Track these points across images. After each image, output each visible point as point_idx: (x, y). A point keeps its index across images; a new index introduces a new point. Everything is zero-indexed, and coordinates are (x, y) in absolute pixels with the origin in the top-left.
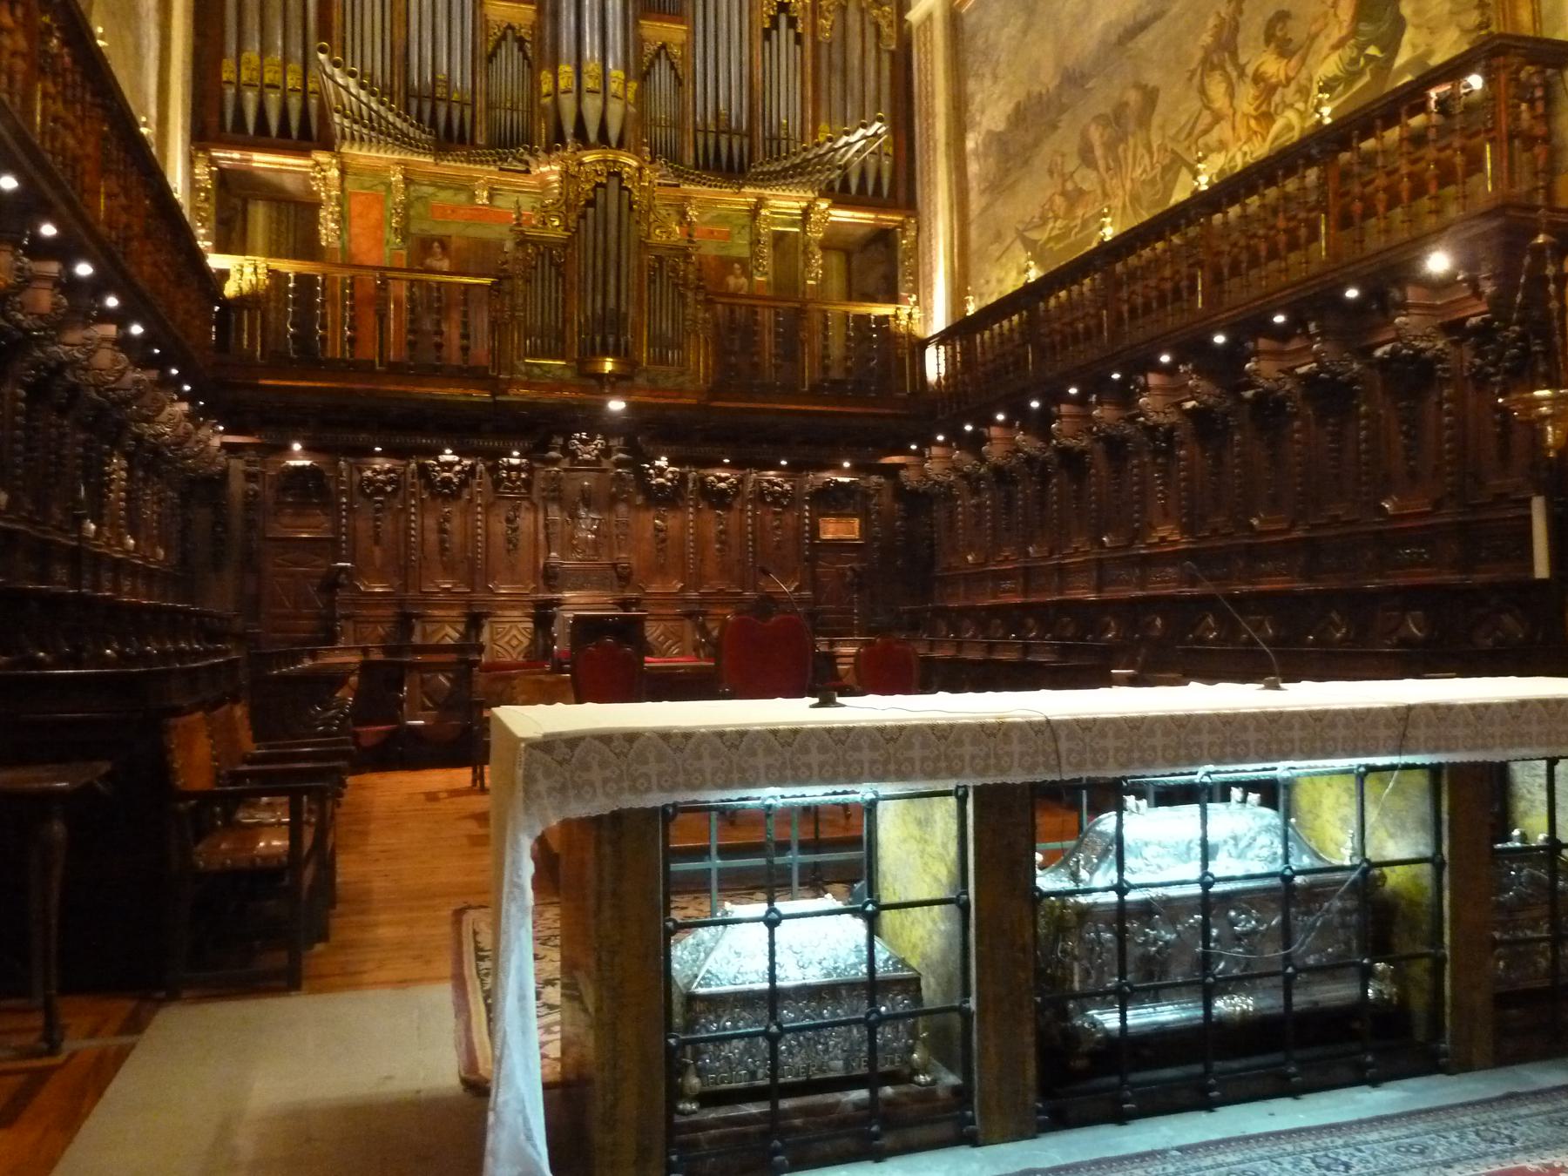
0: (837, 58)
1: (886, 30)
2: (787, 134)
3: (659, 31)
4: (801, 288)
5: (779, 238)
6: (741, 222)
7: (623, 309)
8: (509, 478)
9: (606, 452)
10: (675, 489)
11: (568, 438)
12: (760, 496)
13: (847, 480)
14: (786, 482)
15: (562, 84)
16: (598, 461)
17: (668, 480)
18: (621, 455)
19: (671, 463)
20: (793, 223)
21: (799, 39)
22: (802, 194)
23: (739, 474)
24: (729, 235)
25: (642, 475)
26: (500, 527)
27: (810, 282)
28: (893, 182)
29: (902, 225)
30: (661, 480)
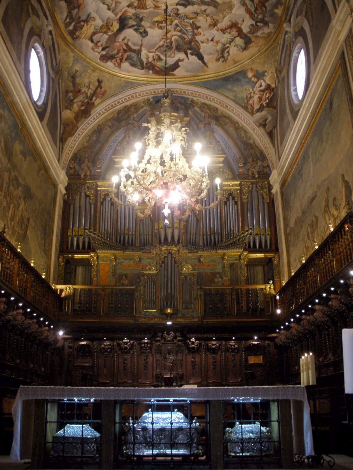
0: (249, 207)
1: (265, 197)
2: (233, 232)
4: (240, 280)
5: (232, 265)
6: (219, 261)
8: (144, 346)
9: (175, 337)
10: (198, 348)
11: (163, 333)
12: (227, 350)
13: (256, 343)
14: (236, 344)
16: (173, 340)
17: (195, 345)
18: (180, 338)
19: (196, 339)
20: (236, 260)
21: (236, 203)
22: (238, 250)
23: (219, 342)
24: (215, 265)
25: (187, 344)
26: (142, 362)
27: (242, 278)
28: (271, 244)
29: (274, 257)
30: (193, 346)
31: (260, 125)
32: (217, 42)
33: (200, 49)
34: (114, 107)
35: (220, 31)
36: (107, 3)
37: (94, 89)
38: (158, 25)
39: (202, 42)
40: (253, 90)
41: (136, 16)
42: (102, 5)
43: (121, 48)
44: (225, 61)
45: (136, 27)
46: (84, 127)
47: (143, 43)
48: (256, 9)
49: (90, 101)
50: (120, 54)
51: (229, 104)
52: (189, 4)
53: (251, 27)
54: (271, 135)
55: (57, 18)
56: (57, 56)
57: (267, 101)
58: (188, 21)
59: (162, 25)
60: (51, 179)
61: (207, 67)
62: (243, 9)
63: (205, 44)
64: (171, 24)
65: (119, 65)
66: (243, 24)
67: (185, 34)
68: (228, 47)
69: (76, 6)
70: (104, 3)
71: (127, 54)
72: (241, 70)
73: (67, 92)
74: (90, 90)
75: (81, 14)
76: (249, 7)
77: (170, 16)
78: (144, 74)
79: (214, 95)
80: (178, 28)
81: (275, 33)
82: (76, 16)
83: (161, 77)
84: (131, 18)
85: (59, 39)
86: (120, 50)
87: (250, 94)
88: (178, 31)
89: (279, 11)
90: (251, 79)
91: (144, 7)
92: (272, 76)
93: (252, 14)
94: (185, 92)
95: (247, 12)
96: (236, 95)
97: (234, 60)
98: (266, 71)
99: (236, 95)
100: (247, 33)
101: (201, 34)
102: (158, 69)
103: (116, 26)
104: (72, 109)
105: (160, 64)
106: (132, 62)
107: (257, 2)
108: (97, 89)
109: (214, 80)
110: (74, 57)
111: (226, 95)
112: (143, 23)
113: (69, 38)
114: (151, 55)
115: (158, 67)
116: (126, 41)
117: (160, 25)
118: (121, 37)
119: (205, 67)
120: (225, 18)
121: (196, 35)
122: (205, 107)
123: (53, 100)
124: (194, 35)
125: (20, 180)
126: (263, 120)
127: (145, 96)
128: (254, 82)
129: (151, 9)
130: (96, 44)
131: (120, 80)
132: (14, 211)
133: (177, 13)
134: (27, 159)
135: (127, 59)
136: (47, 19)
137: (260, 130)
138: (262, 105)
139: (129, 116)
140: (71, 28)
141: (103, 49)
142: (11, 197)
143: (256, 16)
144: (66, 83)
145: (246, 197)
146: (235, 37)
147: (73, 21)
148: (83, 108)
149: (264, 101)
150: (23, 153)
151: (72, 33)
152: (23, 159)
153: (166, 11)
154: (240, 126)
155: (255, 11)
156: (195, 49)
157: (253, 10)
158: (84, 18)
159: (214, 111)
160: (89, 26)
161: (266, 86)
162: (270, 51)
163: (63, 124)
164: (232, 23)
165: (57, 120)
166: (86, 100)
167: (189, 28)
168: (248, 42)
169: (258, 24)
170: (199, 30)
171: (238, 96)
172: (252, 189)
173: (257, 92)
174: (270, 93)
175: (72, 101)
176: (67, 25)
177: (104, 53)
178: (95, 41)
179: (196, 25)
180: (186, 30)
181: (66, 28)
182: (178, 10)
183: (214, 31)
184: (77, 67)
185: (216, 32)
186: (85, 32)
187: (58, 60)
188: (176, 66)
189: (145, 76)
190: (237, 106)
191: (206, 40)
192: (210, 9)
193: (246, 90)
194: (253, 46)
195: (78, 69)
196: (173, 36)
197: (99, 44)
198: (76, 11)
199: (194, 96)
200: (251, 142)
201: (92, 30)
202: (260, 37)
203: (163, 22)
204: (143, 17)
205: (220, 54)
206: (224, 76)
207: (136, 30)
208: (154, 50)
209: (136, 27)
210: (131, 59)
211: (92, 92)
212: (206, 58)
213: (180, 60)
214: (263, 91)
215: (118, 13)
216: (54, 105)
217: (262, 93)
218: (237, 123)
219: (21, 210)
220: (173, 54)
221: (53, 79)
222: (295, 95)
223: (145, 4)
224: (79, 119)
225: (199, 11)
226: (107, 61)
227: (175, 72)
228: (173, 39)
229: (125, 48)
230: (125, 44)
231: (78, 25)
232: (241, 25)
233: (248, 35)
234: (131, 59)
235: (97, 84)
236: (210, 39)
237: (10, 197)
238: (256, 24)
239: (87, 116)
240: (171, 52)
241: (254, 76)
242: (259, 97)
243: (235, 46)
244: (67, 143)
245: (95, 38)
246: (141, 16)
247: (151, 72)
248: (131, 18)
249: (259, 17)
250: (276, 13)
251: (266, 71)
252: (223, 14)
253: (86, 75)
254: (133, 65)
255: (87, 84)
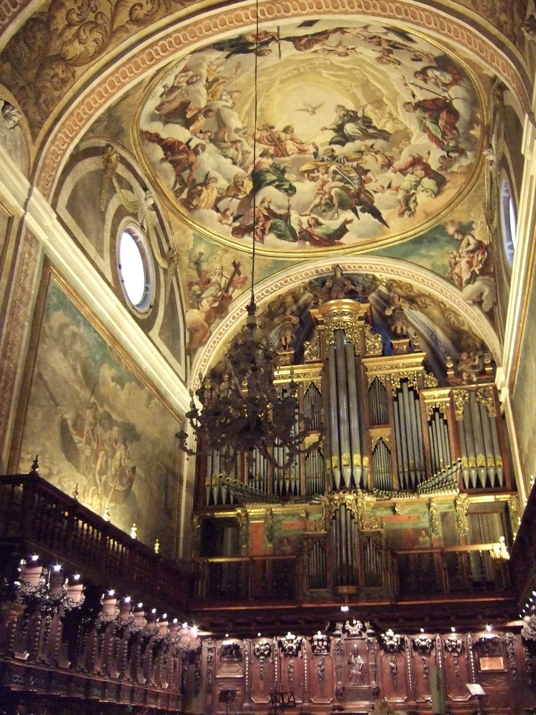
3: (377, 433)
7: (350, 563)
15: (334, 465)
31: (474, 303)
32: (397, 189)
33: (373, 202)
34: (262, 298)
35: (398, 173)
36: (231, 156)
37: (229, 277)
38: (308, 175)
39: (375, 192)
40: (458, 252)
41: (276, 168)
42: (223, 159)
43: (261, 215)
44: (412, 214)
45: (277, 183)
46: (221, 330)
47: (290, 203)
48: (444, 134)
49: (225, 295)
50: (261, 224)
51: (426, 276)
52: (348, 141)
53: (442, 161)
54: (491, 316)
55: (161, 185)
56: (170, 237)
57: (481, 266)
58: (350, 164)
59: (314, 175)
60: (171, 408)
61: (387, 226)
62: (426, 136)
63: (379, 195)
64: (327, 172)
65: (260, 238)
66: (429, 157)
67: (348, 183)
68: (414, 194)
69: (186, 165)
70: (226, 156)
71: (271, 221)
72: (437, 225)
73: (191, 284)
74: (224, 279)
75: (195, 175)
76: (433, 132)
77: (323, 160)
78: (298, 248)
79: (401, 266)
80: (338, 177)
81: (477, 164)
82: (188, 180)
83: (323, 249)
84: (268, 171)
85: (170, 214)
86: (260, 217)
87: (455, 258)
88: (338, 181)
89: (476, 132)
90: (453, 236)
91: (285, 153)
92: (482, 228)
93: (440, 141)
94: (360, 267)
95: (432, 141)
96: (434, 263)
97: (425, 212)
98: (473, 222)
99: (434, 263)
100: (438, 169)
101: (371, 180)
102: (318, 239)
103: (249, 185)
104: (200, 307)
105: (318, 231)
106: (279, 233)
107: (444, 124)
108: (233, 276)
109: (400, 244)
110: (194, 235)
111: (420, 264)
112: (286, 176)
113: (183, 210)
114: (304, 219)
115: (317, 236)
116: (266, 205)
117: (311, 175)
118: (259, 198)
119: (385, 227)
120: (403, 153)
121: (365, 182)
122: (394, 285)
123: (167, 299)
124: (362, 182)
125: (114, 417)
126: (477, 295)
127: (304, 278)
128: (457, 240)
129: (295, 155)
130: (224, 214)
131: (265, 260)
132: (106, 461)
133: (333, 155)
134: (126, 387)
135: (271, 229)
136: (145, 189)
137: (474, 310)
138: (473, 272)
139: (285, 310)
140: (184, 196)
141: (235, 220)
142: (100, 442)
143: (445, 143)
144: (187, 272)
145: (460, 412)
146: (421, 179)
147: (186, 186)
148: (216, 305)
149: (476, 267)
150: (119, 381)
151: (187, 203)
152: (118, 387)
153: (316, 155)
154: (448, 306)
155: (443, 137)
156: (366, 203)
157: (440, 136)
158: (200, 179)
159: (406, 289)
160: (209, 190)
161: (476, 244)
162: (475, 191)
163: (190, 330)
164: (414, 159)
165: (178, 324)
166: (220, 294)
167: (354, 174)
168: (441, 182)
169: (451, 154)
170: (369, 175)
171: (436, 264)
172: (469, 399)
173: (464, 254)
174: (483, 254)
175: (199, 296)
176: (178, 193)
177: (237, 224)
178: (222, 210)
179: (363, 169)
180: (350, 178)
181: (178, 197)
182: (333, 151)
183: (390, 174)
184: (201, 248)
185: (393, 174)
186: (206, 199)
187: (171, 242)
188: (342, 231)
189: (300, 251)
190: (438, 278)
191: (381, 188)
192: (379, 143)
193: (448, 253)
194: (449, 188)
195: (202, 251)
196: (332, 188)
197: (228, 213)
198: (187, 172)
199: (375, 271)
200: (466, 328)
201: (215, 195)
202: (457, 173)
203: (316, 171)
204: (285, 167)
205: (403, 206)
206: (413, 237)
207: (277, 187)
208: (308, 212)
209: (277, 183)
210: (277, 229)
211: (227, 281)
212: (384, 214)
213: (347, 222)
214: (473, 251)
215: (248, 167)
216: (171, 306)
217: (471, 255)
218: (442, 302)
219: (119, 458)
220: (336, 214)
221: (165, 270)
222: (510, 254)
223: (285, 149)
224: (212, 321)
225: (363, 148)
226: (243, 235)
227: (342, 240)
228: (333, 193)
229: (266, 214)
230: (265, 208)
231: (194, 191)
232: (427, 159)
233: (440, 172)
234: (277, 229)
235: (232, 269)
236: (386, 186)
237: (98, 442)
238: (448, 155)
239: (223, 315)
240: (333, 211)
241: (458, 231)
242: (468, 262)
243: (423, 191)
244: (197, 356)
245: (222, 205)
246: (282, 167)
247: (308, 243)
248: (268, 171)
249: (451, 144)
250: (472, 136)
251: (473, 222)
252: (398, 148)
253: (215, 259)
254: (281, 236)
255: (218, 271)
